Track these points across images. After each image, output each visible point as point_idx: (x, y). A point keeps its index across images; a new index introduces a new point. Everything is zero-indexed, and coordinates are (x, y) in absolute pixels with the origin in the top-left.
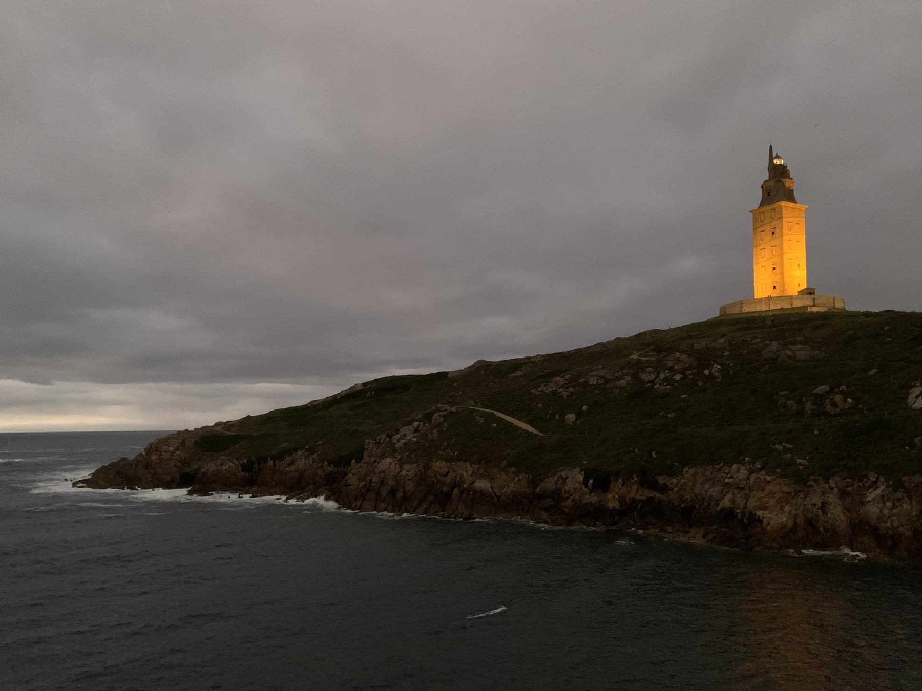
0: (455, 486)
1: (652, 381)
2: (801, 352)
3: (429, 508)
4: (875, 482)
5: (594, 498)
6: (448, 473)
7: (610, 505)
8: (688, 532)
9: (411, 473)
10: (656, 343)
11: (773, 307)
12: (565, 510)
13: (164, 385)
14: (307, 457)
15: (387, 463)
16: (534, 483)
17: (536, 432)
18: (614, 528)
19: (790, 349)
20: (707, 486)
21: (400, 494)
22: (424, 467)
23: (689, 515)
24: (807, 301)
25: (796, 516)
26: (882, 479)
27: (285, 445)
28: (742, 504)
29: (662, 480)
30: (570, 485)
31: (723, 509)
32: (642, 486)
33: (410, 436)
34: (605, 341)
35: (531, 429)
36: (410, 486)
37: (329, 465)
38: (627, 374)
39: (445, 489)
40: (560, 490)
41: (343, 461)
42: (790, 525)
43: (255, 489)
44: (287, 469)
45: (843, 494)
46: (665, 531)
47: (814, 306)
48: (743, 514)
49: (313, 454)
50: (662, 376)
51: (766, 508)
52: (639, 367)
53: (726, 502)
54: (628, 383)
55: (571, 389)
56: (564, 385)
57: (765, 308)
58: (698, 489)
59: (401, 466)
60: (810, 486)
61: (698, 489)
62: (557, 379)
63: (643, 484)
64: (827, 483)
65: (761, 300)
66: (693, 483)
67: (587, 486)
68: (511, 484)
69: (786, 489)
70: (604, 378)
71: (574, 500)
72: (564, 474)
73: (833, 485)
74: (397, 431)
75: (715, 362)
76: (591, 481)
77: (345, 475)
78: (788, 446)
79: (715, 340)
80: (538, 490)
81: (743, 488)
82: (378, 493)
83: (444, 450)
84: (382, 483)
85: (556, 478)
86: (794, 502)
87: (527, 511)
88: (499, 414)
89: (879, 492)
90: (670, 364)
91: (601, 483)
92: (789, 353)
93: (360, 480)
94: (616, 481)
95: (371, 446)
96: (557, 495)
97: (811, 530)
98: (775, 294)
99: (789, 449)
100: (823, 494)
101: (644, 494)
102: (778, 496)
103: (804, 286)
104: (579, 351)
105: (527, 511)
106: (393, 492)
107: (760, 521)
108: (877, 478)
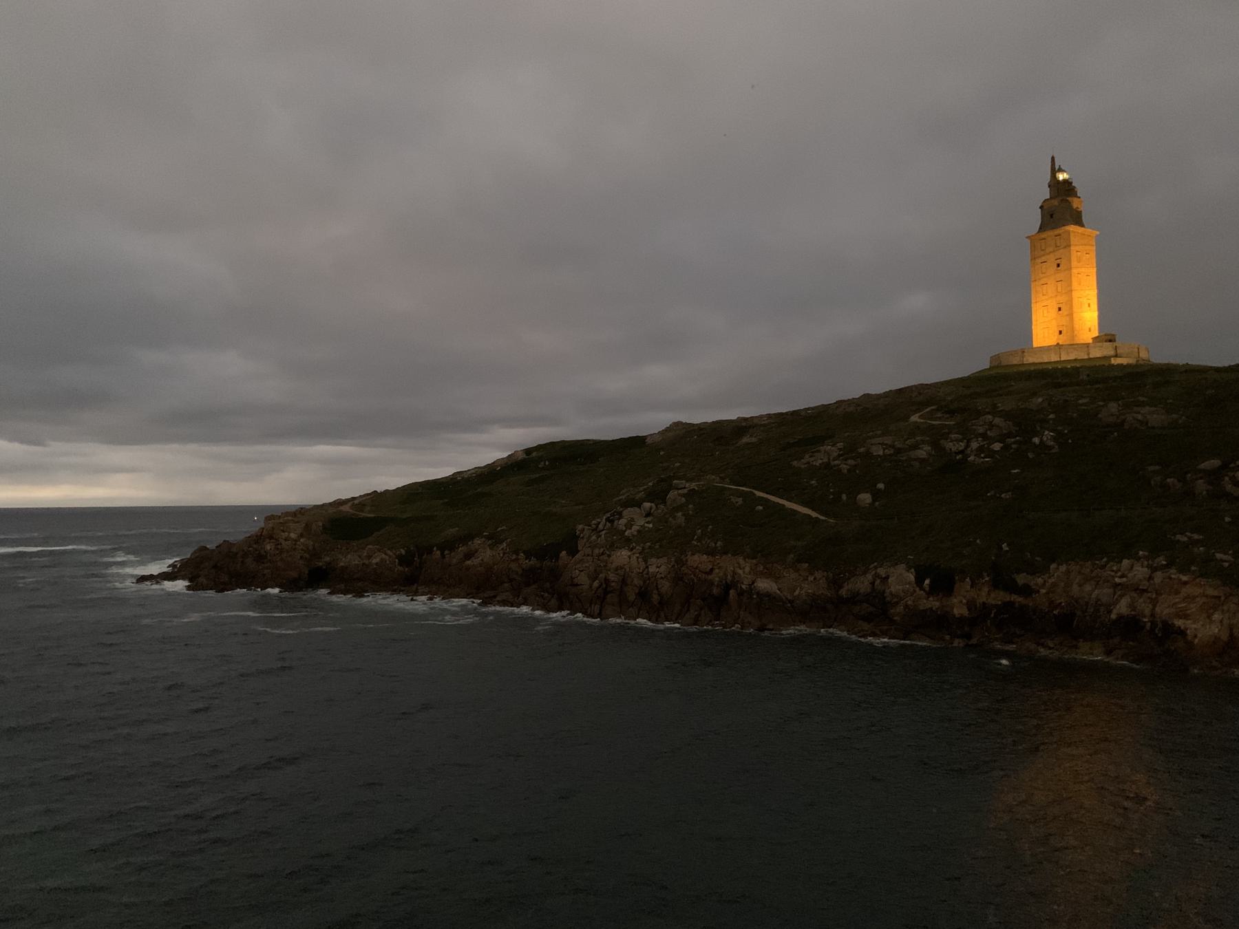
0: (727, 587)
1: (962, 452)
2: (1155, 417)
3: (699, 615)
5: (933, 603)
6: (712, 570)
7: (956, 611)
8: (1076, 647)
13: (193, 447)
14: (492, 547)
15: (622, 556)
20: (1088, 588)
21: (655, 598)
24: (1105, 350)
28: (1147, 612)
29: (1021, 579)
30: (894, 587)
35: (814, 514)
36: (665, 586)
38: (923, 442)
46: (1043, 645)
47: (1116, 356)
49: (501, 542)
50: (974, 445)
51: (1186, 617)
53: (1122, 607)
56: (840, 456)
57: (1054, 358)
58: (1075, 589)
59: (646, 561)
61: (1075, 589)
63: (996, 585)
65: (1041, 349)
66: (1063, 582)
67: (922, 588)
68: (805, 584)
69: (1210, 592)
70: (893, 446)
71: (906, 606)
72: (882, 572)
74: (620, 516)
76: (927, 582)
78: (1196, 536)
84: (624, 582)
85: (869, 577)
86: (1225, 608)
88: (759, 494)
90: (981, 430)
91: (944, 584)
92: (1140, 417)
94: (963, 580)
95: (587, 533)
99: (1198, 541)
101: (998, 598)
106: (643, 595)
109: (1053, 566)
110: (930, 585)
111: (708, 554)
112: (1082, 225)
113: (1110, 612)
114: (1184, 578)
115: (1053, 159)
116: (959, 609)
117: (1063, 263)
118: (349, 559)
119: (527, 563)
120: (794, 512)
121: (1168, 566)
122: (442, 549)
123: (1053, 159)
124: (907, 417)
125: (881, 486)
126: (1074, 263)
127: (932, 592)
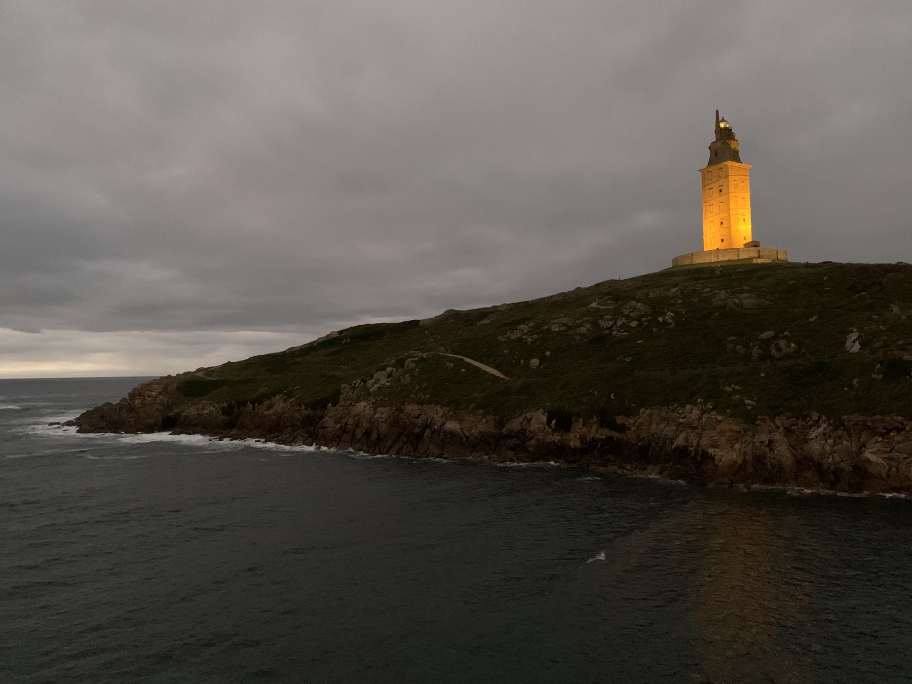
0: (427, 427)
1: (610, 328)
2: (748, 300)
3: (402, 448)
4: (817, 421)
5: (556, 438)
6: (419, 416)
7: (572, 444)
8: (645, 469)
9: (385, 416)
10: (613, 293)
11: (721, 259)
12: (530, 449)
16: (500, 424)
17: (502, 376)
18: (575, 465)
19: (738, 298)
20: (662, 426)
21: (374, 436)
22: (397, 410)
23: (645, 453)
24: (753, 253)
25: (745, 453)
26: (824, 418)
27: (263, 390)
28: (695, 443)
29: (620, 420)
30: (534, 426)
31: (677, 447)
32: (602, 426)
33: (384, 381)
34: (566, 290)
36: (384, 428)
37: (306, 409)
39: (417, 430)
40: (525, 430)
41: (320, 405)
42: (740, 461)
43: (234, 431)
44: (267, 412)
45: (788, 431)
46: (623, 468)
47: (759, 257)
48: (696, 451)
50: (619, 323)
51: (717, 446)
52: (598, 314)
53: (680, 441)
54: (588, 330)
55: (535, 336)
57: (714, 259)
59: (375, 409)
60: (758, 425)
62: (522, 326)
63: (603, 424)
64: (774, 422)
65: (710, 252)
66: (650, 423)
68: (478, 425)
69: (735, 428)
70: (566, 325)
72: (528, 415)
73: (779, 424)
75: (668, 310)
76: (554, 422)
77: (321, 418)
78: (737, 387)
79: (668, 290)
80: (504, 430)
81: (696, 428)
82: (354, 434)
83: (416, 393)
84: (357, 425)
87: (495, 450)
89: (821, 430)
90: (627, 312)
92: (737, 301)
93: (336, 423)
96: (522, 435)
97: (758, 466)
98: (722, 246)
100: (770, 432)
101: (604, 433)
102: (728, 434)
103: (749, 239)
104: (542, 300)
105: (495, 450)
106: (368, 434)
107: (712, 458)
108: (820, 417)
109: (642, 410)
110: (556, 424)
111: (419, 404)
112: (739, 161)
113: (672, 444)
114: (720, 418)
115: (717, 112)
116: (574, 442)
117: (724, 189)
118: (191, 411)
119: (306, 412)
120: (485, 373)
121: (713, 409)
122: (253, 403)
123: (717, 112)
124: (589, 304)
125: (548, 353)
126: (731, 189)
127: (557, 429)
